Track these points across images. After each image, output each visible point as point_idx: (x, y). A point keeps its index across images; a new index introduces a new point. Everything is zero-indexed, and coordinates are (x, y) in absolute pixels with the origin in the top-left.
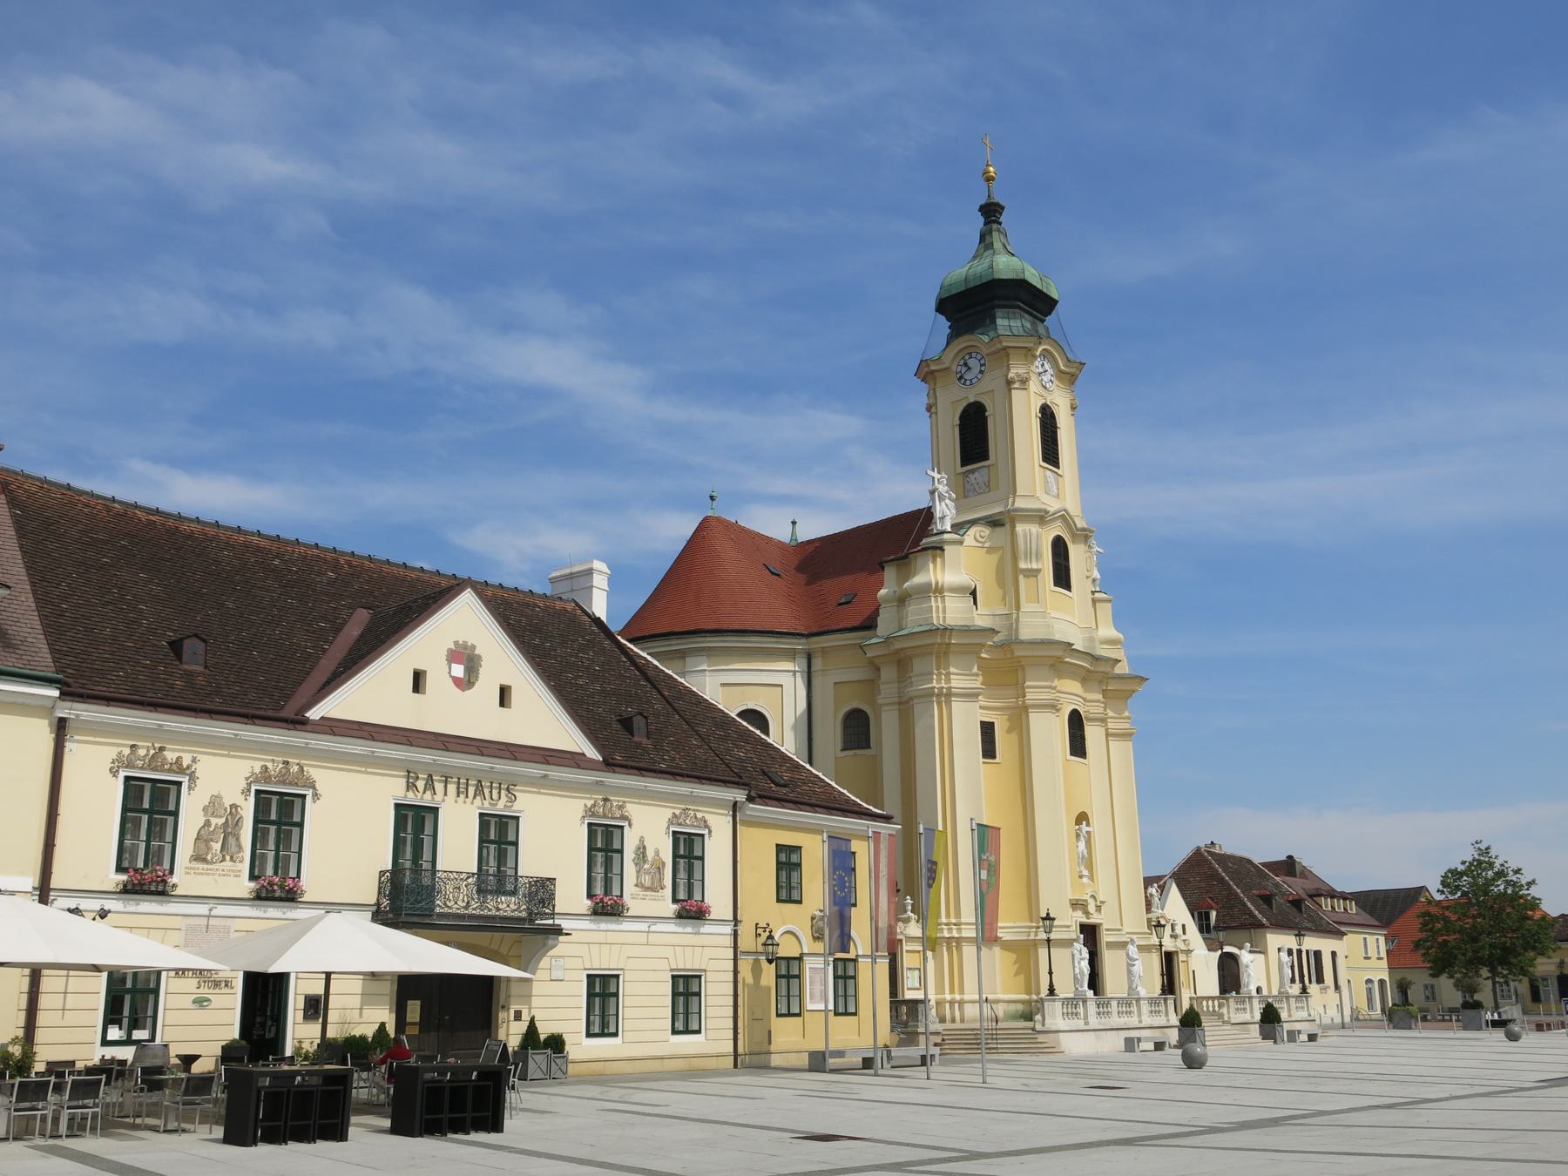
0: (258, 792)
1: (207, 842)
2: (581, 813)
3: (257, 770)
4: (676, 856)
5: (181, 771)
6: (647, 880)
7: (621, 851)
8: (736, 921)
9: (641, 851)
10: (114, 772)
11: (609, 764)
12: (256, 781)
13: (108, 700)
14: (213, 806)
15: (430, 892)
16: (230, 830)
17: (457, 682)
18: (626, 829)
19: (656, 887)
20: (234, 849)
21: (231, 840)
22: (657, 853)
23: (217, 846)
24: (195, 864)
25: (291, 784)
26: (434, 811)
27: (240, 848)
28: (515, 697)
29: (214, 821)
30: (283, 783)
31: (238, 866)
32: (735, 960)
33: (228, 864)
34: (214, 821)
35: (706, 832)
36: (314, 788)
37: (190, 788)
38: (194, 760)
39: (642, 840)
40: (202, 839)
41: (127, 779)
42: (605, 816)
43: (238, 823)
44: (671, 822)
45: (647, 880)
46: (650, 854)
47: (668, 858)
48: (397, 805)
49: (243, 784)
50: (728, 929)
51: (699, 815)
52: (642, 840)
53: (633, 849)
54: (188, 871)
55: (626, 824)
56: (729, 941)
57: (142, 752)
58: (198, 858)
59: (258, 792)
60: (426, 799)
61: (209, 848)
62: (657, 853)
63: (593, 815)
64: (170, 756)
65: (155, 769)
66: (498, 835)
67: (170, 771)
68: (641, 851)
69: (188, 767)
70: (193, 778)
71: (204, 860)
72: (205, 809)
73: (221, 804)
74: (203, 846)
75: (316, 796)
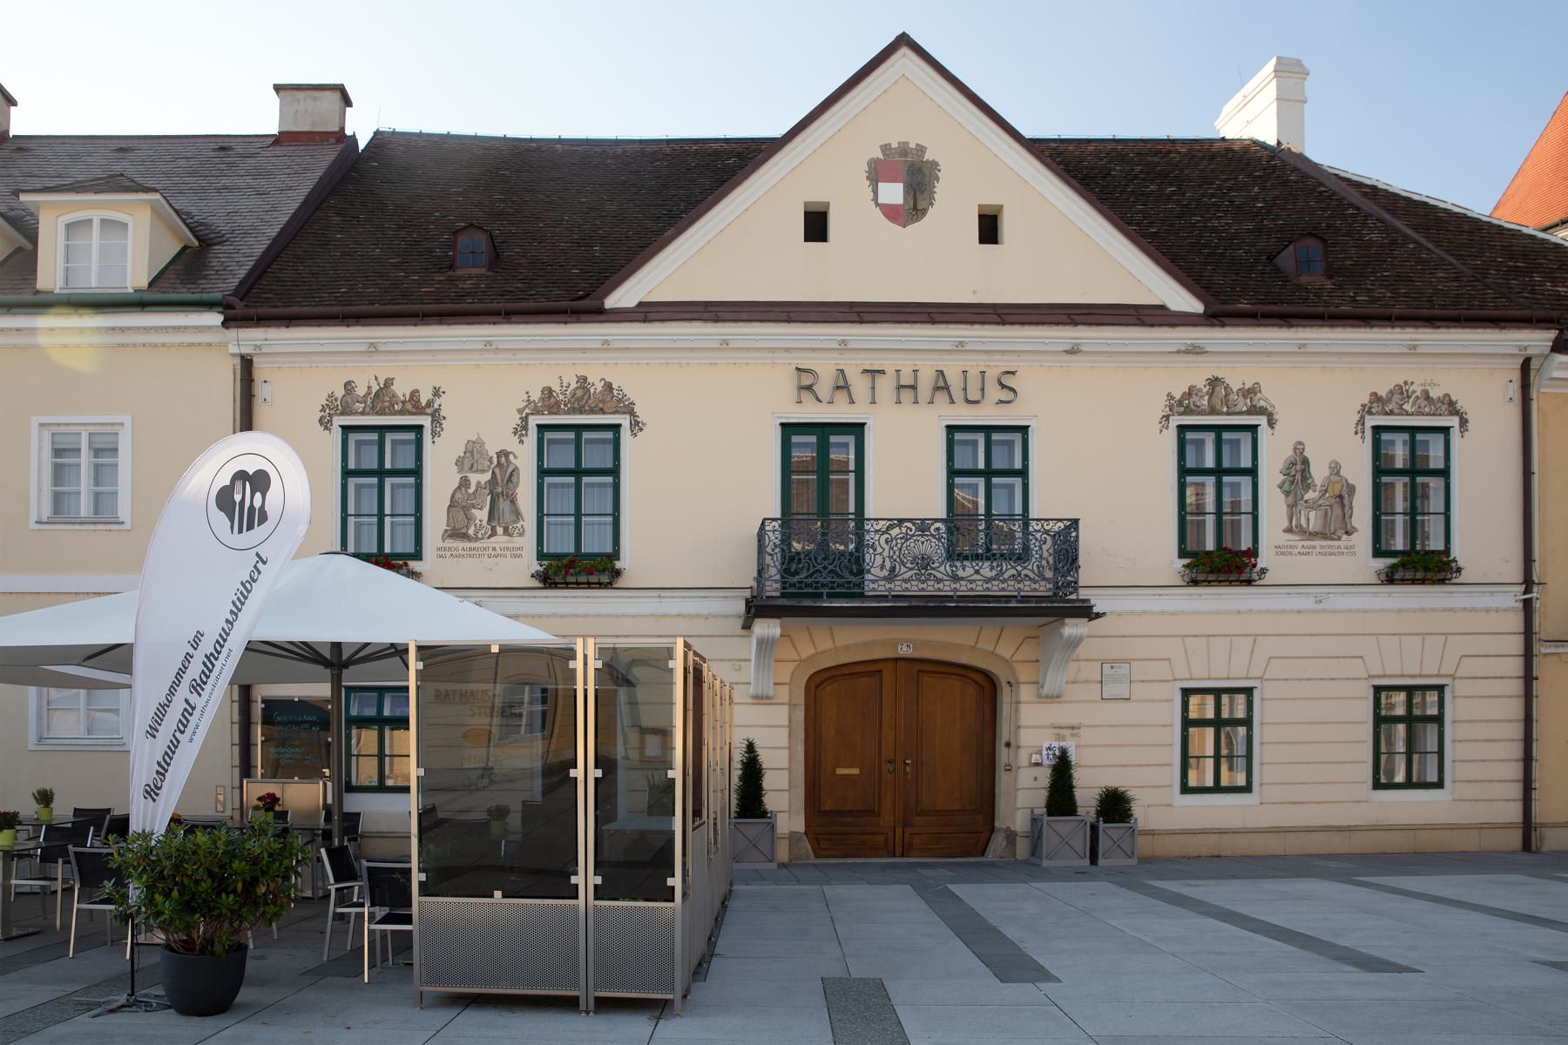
2: (1160, 408)
3: (536, 396)
5: (419, 410)
6: (1313, 520)
7: (1252, 472)
8: (1528, 583)
9: (1298, 473)
10: (325, 423)
11: (1215, 317)
12: (537, 412)
13: (290, 320)
14: (471, 456)
15: (856, 563)
17: (891, 213)
18: (1264, 433)
19: (1335, 527)
20: (508, 516)
21: (503, 504)
22: (1335, 469)
25: (592, 411)
26: (857, 429)
27: (517, 514)
28: (1007, 227)
29: (474, 478)
30: (581, 411)
32: (1528, 656)
34: (474, 478)
35: (1453, 422)
36: (632, 413)
37: (434, 433)
38: (437, 392)
39: (1299, 448)
40: (459, 505)
41: (346, 429)
42: (1213, 411)
43: (512, 478)
44: (1367, 410)
45: (1313, 520)
46: (1319, 473)
47: (1360, 474)
48: (782, 425)
50: (1511, 599)
51: (1434, 394)
52: (1299, 448)
53: (1280, 464)
54: (441, 553)
55: (1262, 421)
56: (1516, 622)
57: (361, 391)
60: (840, 413)
61: (470, 519)
62: (1335, 469)
63: (1188, 411)
64: (401, 389)
65: (382, 413)
66: (988, 457)
67: (402, 412)
68: (1298, 473)
69: (429, 404)
70: (437, 418)
73: (483, 453)
75: (636, 426)
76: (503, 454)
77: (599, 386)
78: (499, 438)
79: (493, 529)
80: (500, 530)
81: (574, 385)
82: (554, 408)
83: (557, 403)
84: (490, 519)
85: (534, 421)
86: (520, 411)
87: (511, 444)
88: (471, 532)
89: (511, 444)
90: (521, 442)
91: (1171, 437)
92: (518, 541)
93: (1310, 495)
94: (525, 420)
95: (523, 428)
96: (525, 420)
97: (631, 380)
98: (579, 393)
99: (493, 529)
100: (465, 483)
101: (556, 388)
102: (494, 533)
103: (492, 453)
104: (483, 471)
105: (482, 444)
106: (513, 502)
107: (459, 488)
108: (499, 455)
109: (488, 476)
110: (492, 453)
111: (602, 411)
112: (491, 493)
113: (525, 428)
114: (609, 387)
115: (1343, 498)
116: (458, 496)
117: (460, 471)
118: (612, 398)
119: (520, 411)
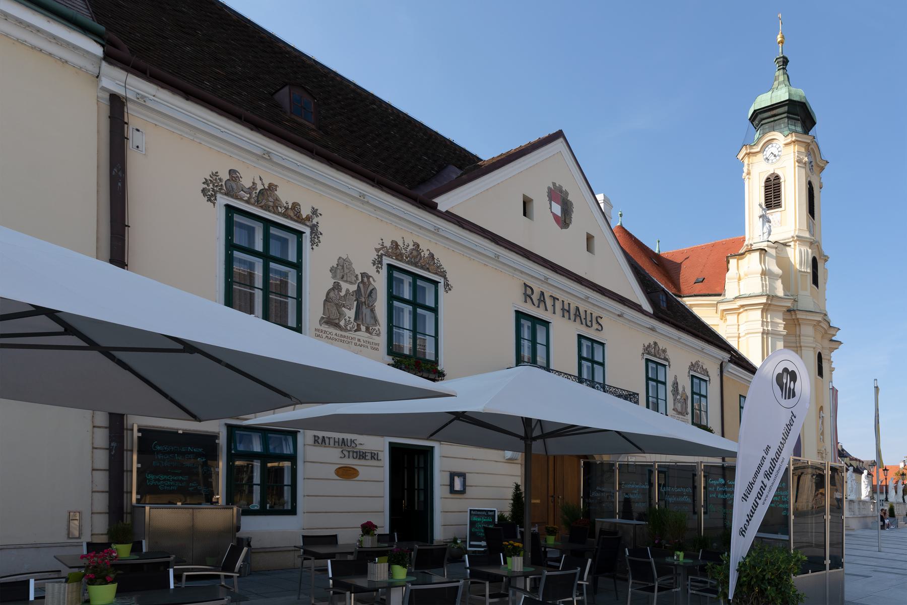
1: (339, 306)
4: (693, 393)
7: (664, 383)
16: (363, 298)
22: (684, 388)
24: (325, 327)
30: (415, 265)
39: (676, 377)
40: (332, 301)
43: (372, 293)
45: (679, 409)
52: (676, 377)
61: (341, 315)
62: (684, 388)
71: (337, 326)
74: (334, 310)
77: (427, 254)
81: (411, 247)
82: (399, 257)
83: (401, 254)
84: (356, 319)
85: (386, 260)
87: (371, 270)
88: (342, 323)
89: (371, 270)
90: (378, 271)
91: (644, 361)
92: (376, 339)
93: (679, 397)
97: (446, 258)
98: (415, 253)
101: (400, 243)
111: (428, 270)
112: (357, 300)
113: (380, 262)
114: (432, 256)
115: (685, 400)
118: (431, 263)
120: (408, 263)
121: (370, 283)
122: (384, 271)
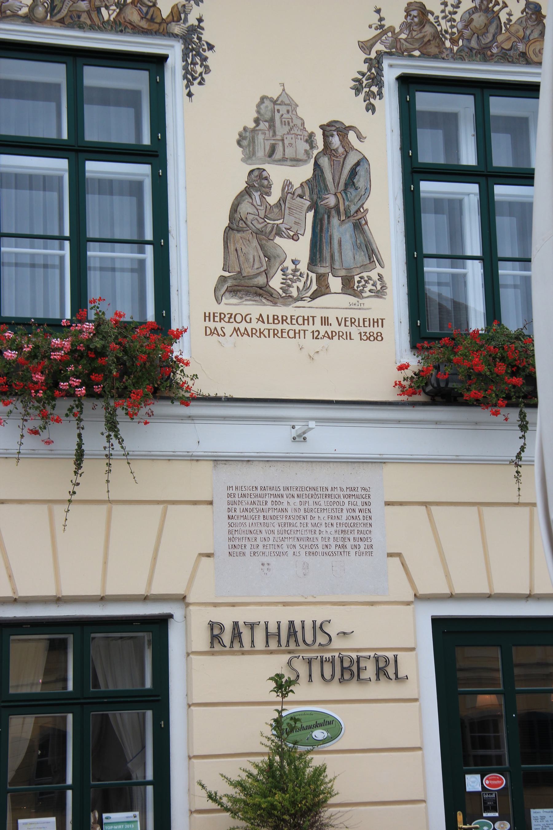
0: (407, 82)
1: (264, 236)
3: (395, 18)
12: (397, 50)
14: (269, 128)
16: (333, 194)
20: (349, 255)
21: (340, 231)
23: (297, 250)
24: (232, 305)
25: (505, 57)
27: (371, 253)
30: (483, 55)
31: (373, 307)
33: (336, 303)
34: (278, 175)
43: (355, 178)
49: (357, 63)
58: (240, 284)
59: (407, 82)
61: (271, 257)
71: (263, 293)
72: (246, 140)
73: (295, 125)
74: (252, 249)
76: (333, 129)
78: (326, 94)
79: (321, 279)
80: (335, 283)
82: (432, 46)
83: (438, 36)
86: (365, 46)
87: (349, 109)
88: (276, 283)
89: (349, 109)
90: (371, 108)
94: (375, 64)
95: (368, 84)
96: (375, 64)
98: (479, 19)
99: (321, 279)
100: (257, 183)
102: (323, 290)
103: (313, 126)
104: (296, 161)
105: (292, 106)
106: (359, 227)
107: (247, 192)
108: (328, 129)
109: (305, 172)
110: (313, 126)
112: (314, 206)
113: (377, 80)
116: (245, 208)
117: (249, 157)
119: (365, 46)
120: (459, 57)
121: (348, 148)
122: (389, 104)
